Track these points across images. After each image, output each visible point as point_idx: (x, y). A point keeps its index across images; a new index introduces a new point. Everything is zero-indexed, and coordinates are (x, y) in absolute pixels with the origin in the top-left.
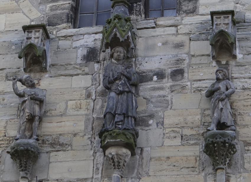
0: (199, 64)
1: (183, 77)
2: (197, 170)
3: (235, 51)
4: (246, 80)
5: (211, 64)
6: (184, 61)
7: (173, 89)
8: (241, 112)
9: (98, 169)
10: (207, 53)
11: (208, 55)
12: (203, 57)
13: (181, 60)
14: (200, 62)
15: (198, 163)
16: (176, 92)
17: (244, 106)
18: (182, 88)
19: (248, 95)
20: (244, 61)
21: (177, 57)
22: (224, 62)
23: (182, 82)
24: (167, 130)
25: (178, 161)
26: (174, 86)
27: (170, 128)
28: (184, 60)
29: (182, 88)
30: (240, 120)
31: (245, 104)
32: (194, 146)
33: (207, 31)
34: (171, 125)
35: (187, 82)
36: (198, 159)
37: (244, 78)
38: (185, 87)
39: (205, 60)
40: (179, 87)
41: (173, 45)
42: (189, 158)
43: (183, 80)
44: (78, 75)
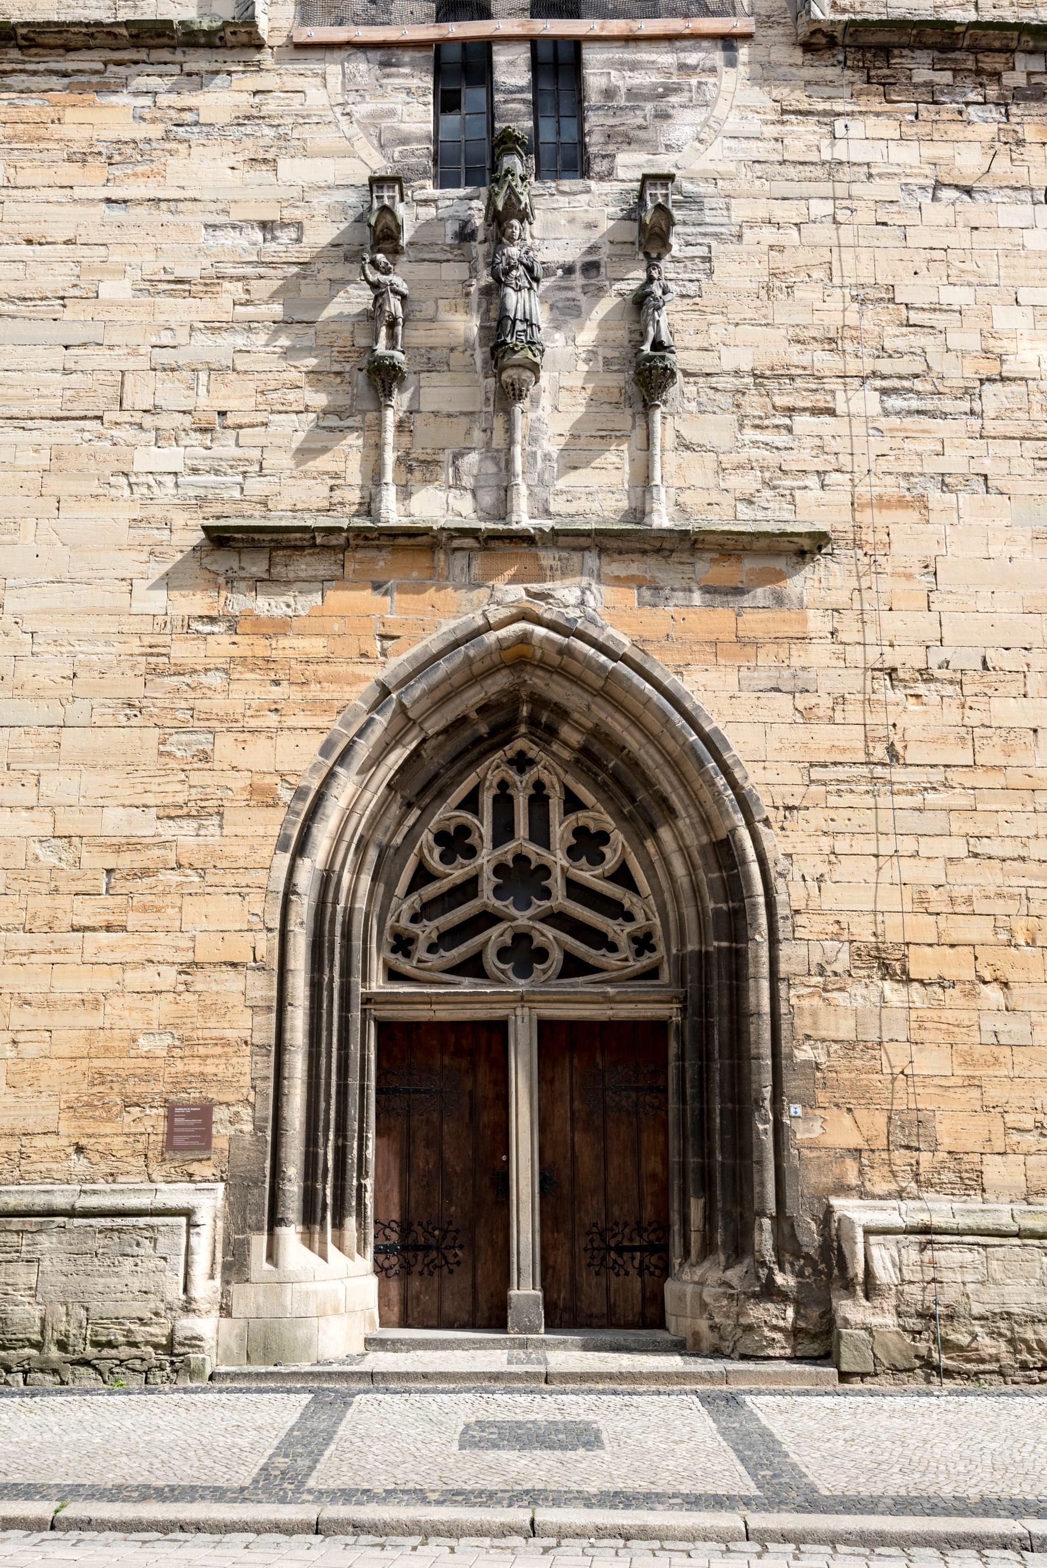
1: (598, 274)
9: (488, 399)
11: (633, 243)
22: (654, 255)
24: (580, 350)
39: (627, 249)
44: (448, 261)
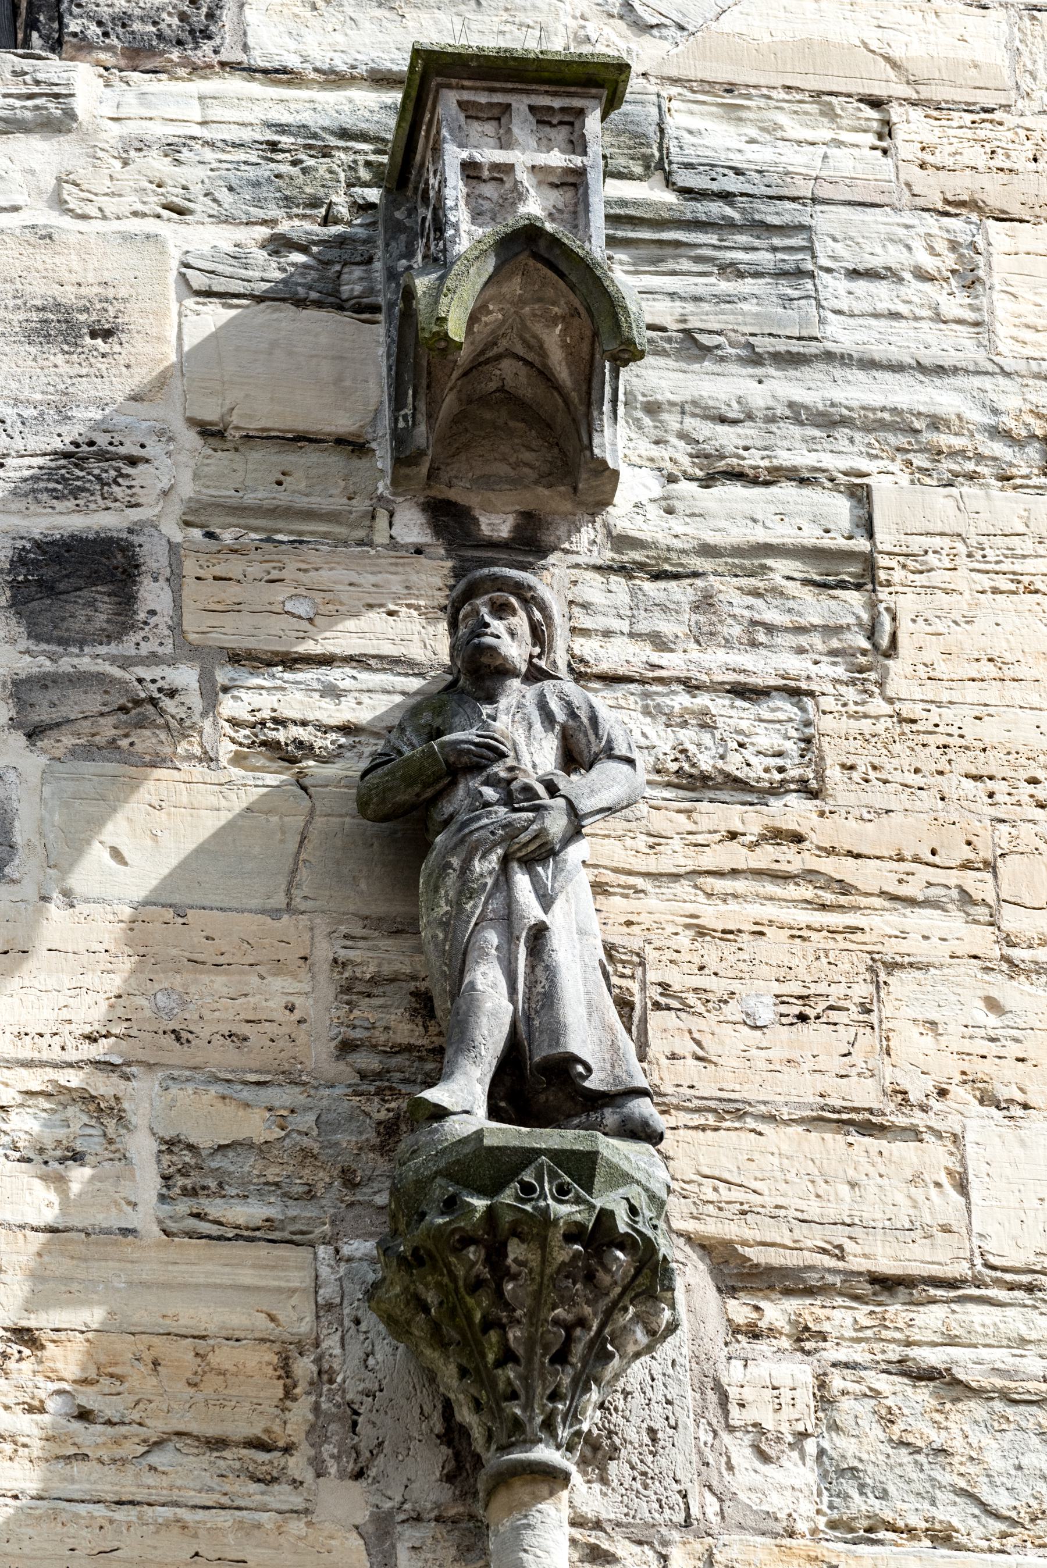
0: (273, 512)
2: (297, 1465)
3: (607, 431)
4: (703, 700)
5: (382, 521)
6: (127, 470)
7: (43, 714)
8: (677, 980)
10: (343, 423)
12: (310, 458)
13: (103, 456)
14: (282, 497)
15: (301, 1411)
16: (69, 741)
17: (702, 932)
18: (123, 709)
19: (733, 835)
20: (679, 529)
21: (63, 429)
23: (126, 663)
25: (120, 1378)
26: (45, 687)
27: (27, 1064)
28: (133, 461)
29: (123, 709)
30: (673, 1057)
31: (712, 915)
32: (262, 1251)
33: (325, 222)
34: (43, 1042)
35: (171, 662)
36: (304, 1367)
37: (691, 686)
38: (153, 701)
40: (93, 702)
41: (22, 316)
42: (223, 1357)
43: (135, 637)
